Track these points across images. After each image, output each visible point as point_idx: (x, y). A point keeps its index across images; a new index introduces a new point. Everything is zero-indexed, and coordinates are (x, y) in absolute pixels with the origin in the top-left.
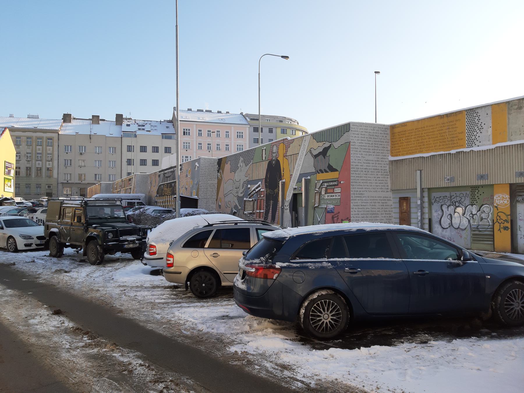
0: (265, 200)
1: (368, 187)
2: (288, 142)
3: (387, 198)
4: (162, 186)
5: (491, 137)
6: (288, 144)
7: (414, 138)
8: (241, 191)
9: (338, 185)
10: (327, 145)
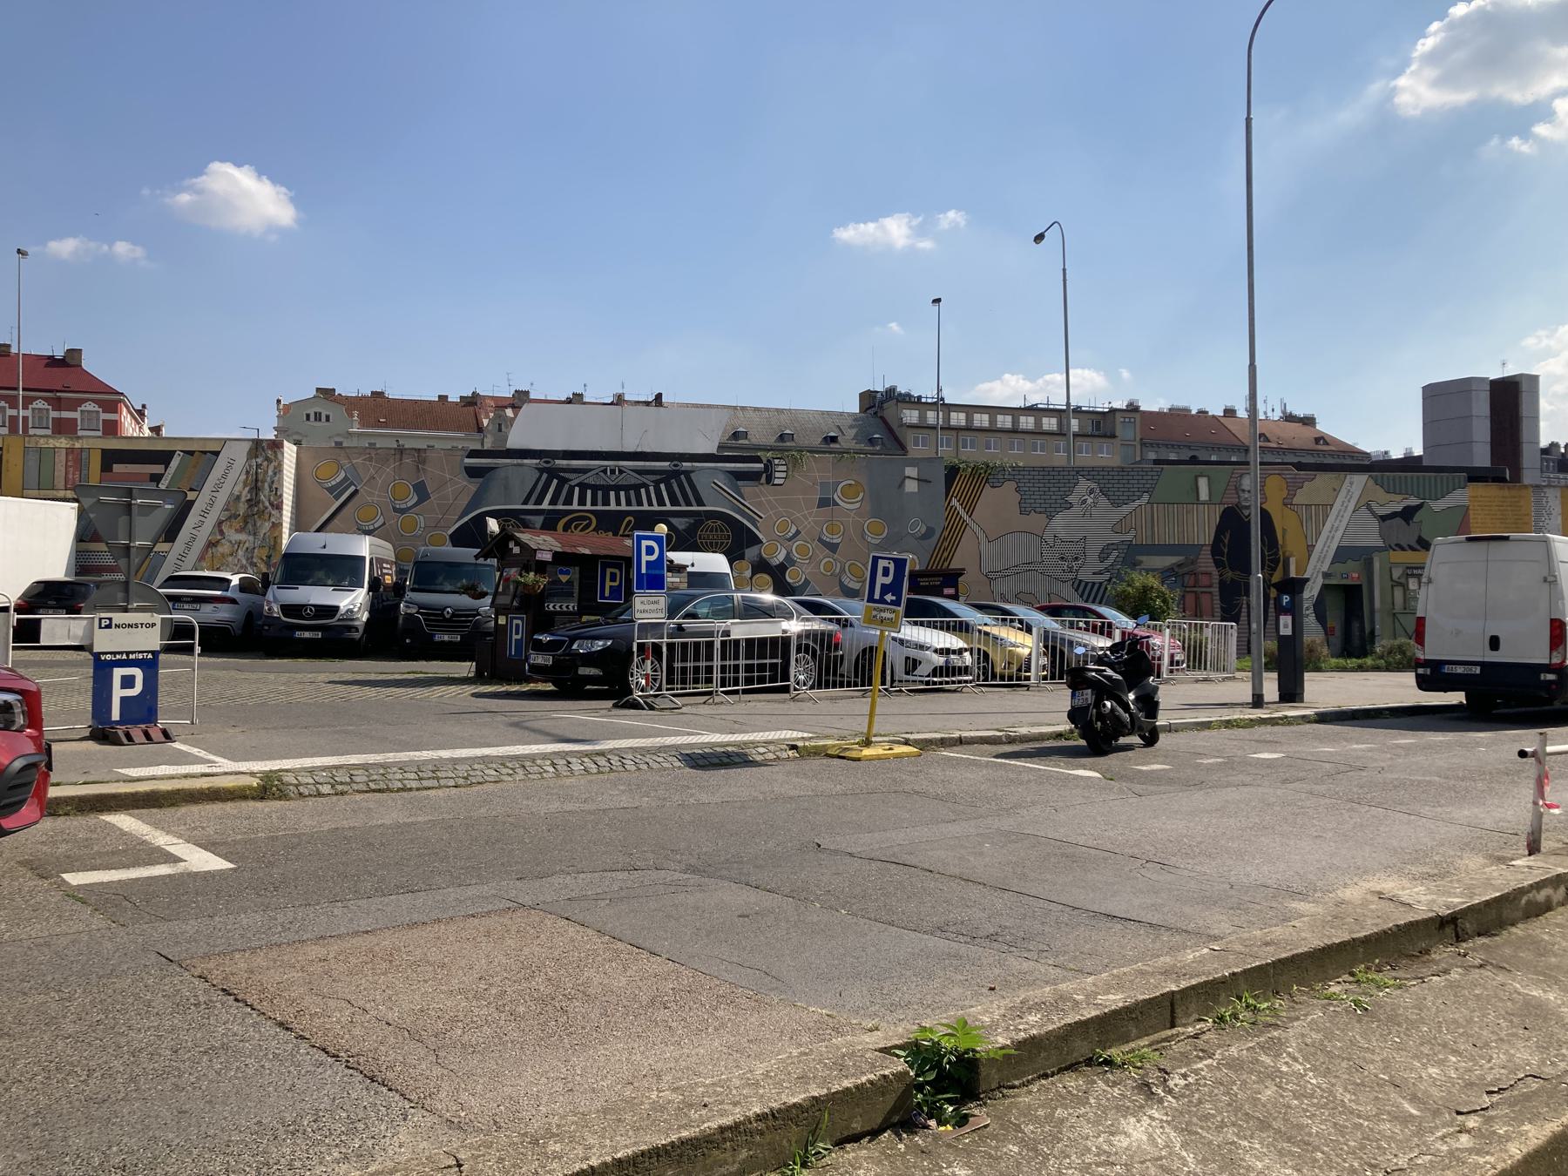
10: (1414, 501)
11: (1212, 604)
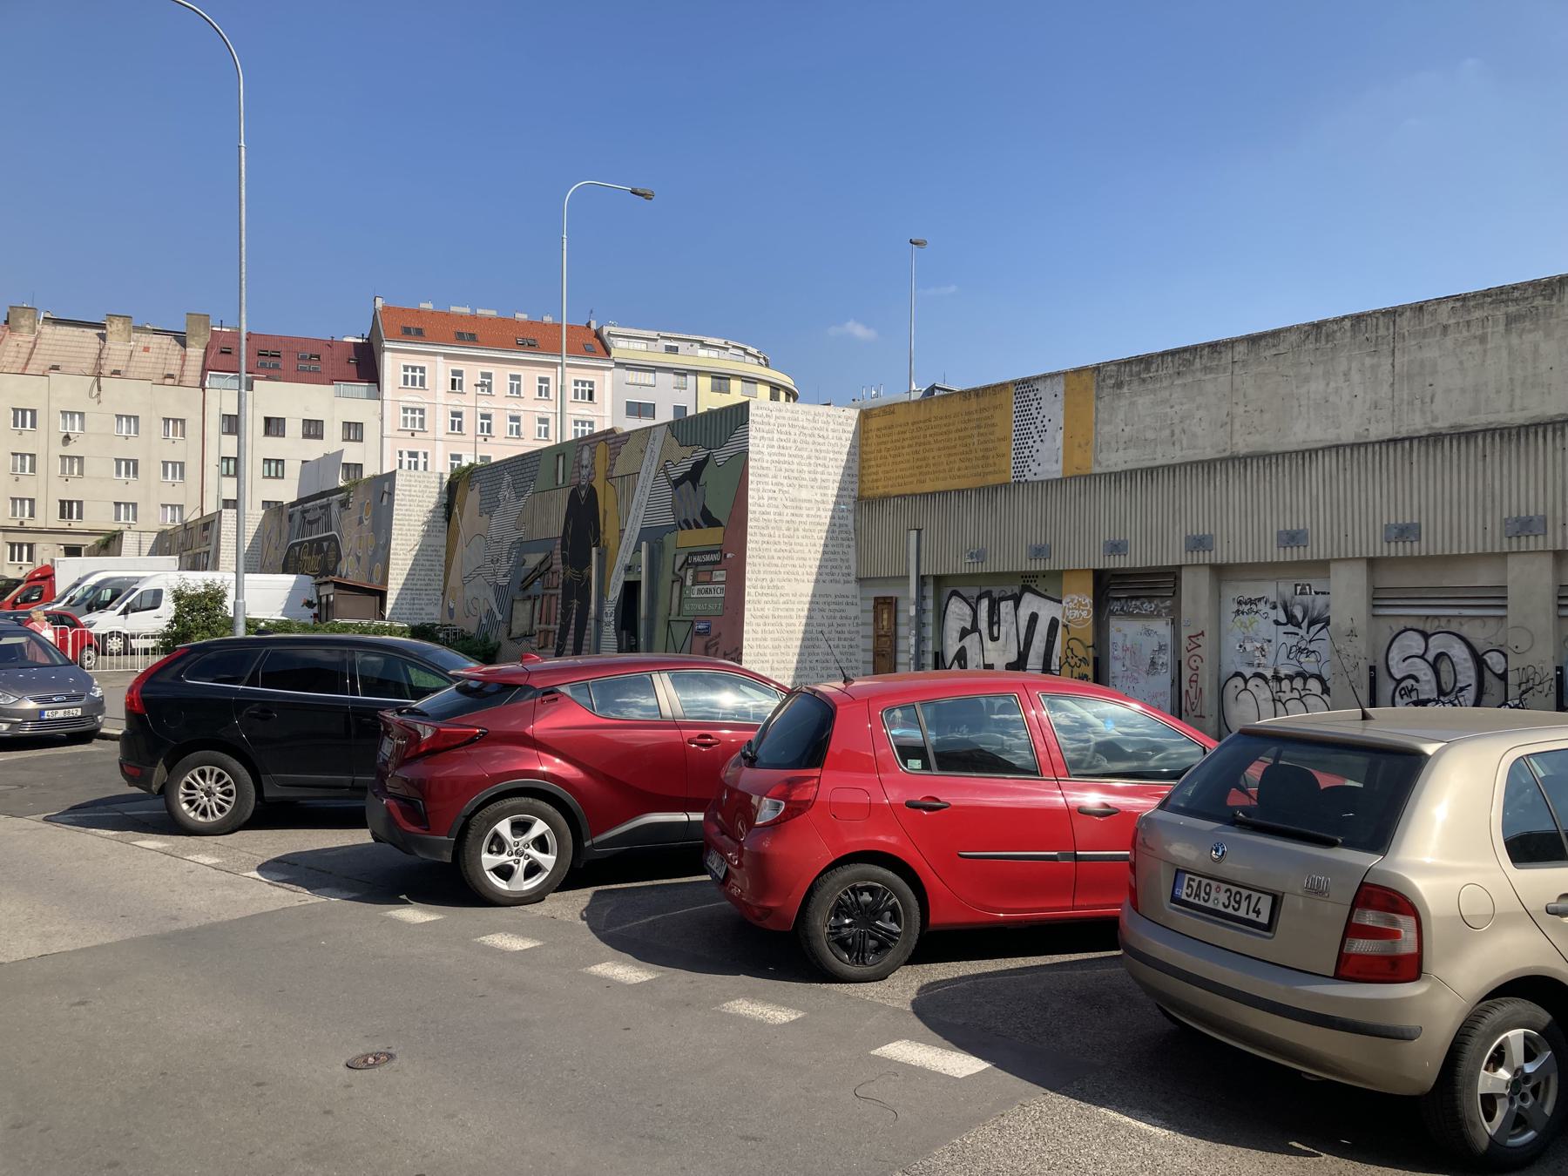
0: (560, 596)
1: (795, 570)
2: (617, 440)
3: (845, 600)
4: (297, 548)
5: (1061, 452)
6: (618, 445)
7: (910, 446)
8: (504, 571)
9: (719, 563)
10: (701, 454)
11: (557, 608)
